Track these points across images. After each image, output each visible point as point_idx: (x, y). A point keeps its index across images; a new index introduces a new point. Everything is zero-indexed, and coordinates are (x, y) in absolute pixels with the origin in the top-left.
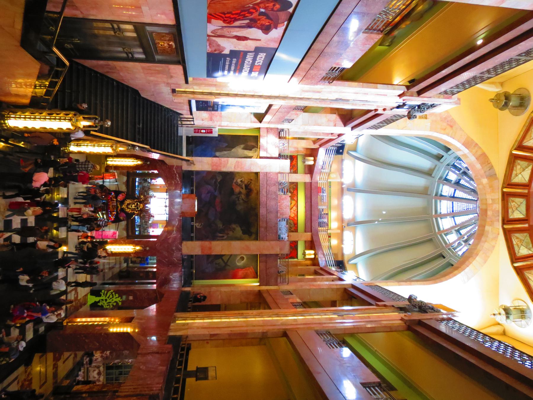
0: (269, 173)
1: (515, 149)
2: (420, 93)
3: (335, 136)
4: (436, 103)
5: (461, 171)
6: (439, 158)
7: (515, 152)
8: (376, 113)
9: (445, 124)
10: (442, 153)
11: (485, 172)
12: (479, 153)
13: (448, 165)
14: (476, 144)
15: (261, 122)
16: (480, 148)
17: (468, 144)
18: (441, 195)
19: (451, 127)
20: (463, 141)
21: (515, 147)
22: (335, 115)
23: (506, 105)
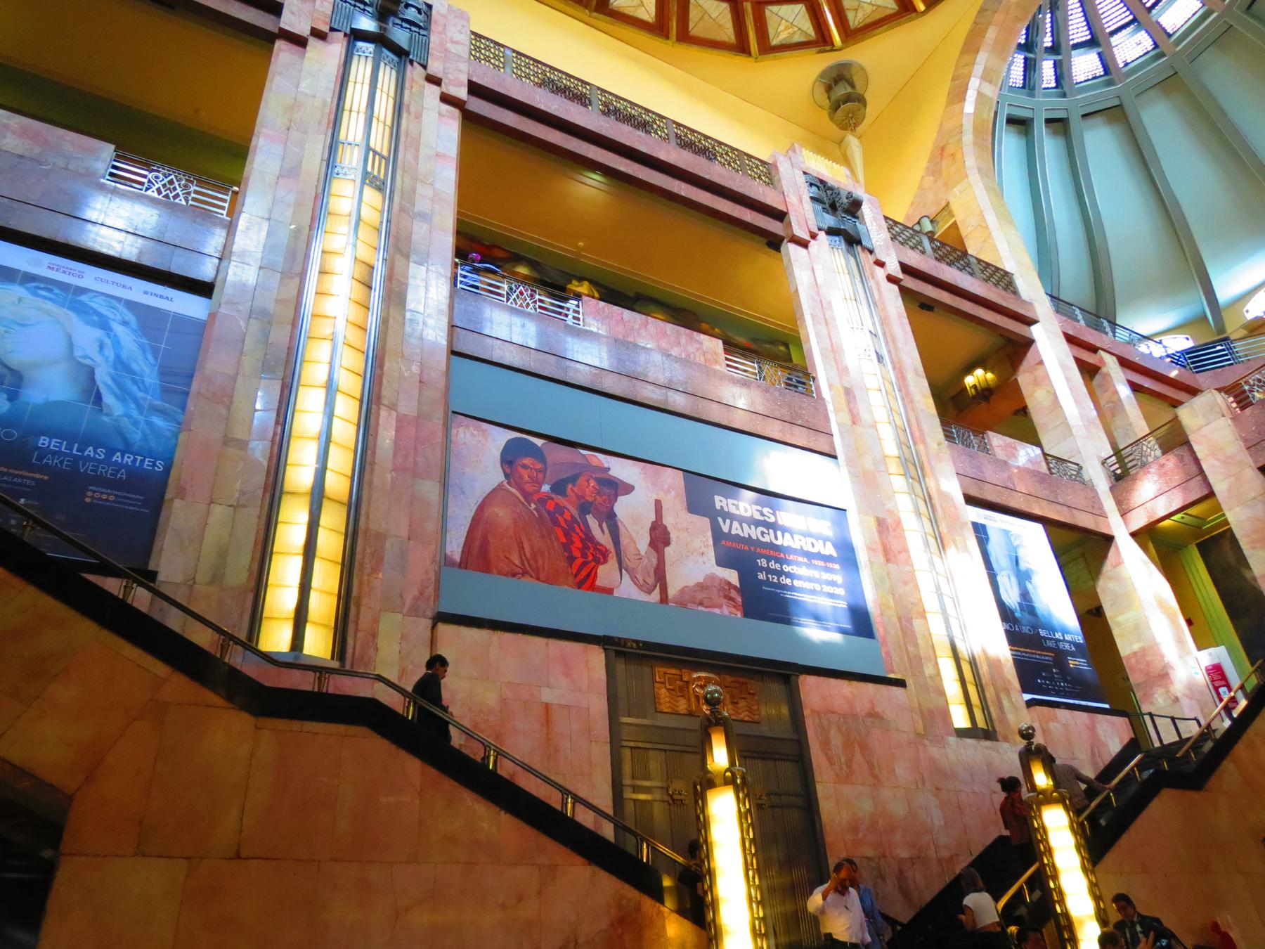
0: (1245, 440)
1: (915, 10)
2: (780, 216)
3: (1102, 360)
4: (801, 180)
5: (1059, 57)
6: (1059, 125)
7: (922, 7)
8: (901, 276)
9: (944, 163)
10: (1040, 128)
11: (995, 12)
12: (966, 58)
13: (1064, 95)
14: (953, 79)
15: (1109, 539)
16: (957, 68)
17: (958, 95)
18: (1156, 46)
19: (943, 149)
20: (957, 106)
21: (913, 15)
22: (1019, 379)
23: (848, 99)
